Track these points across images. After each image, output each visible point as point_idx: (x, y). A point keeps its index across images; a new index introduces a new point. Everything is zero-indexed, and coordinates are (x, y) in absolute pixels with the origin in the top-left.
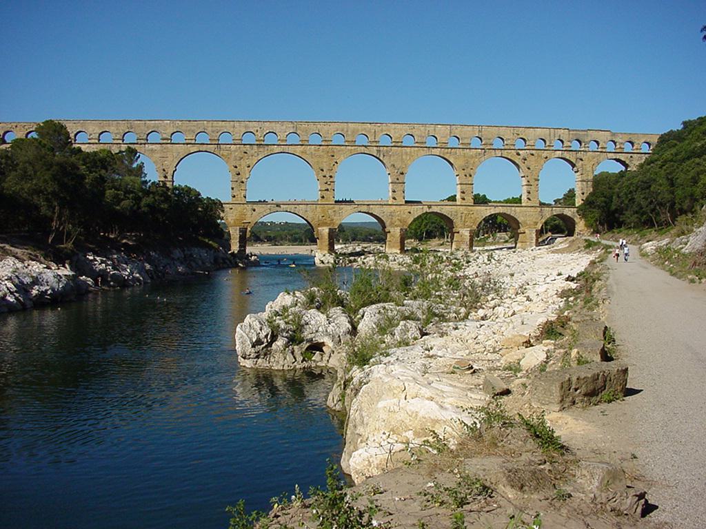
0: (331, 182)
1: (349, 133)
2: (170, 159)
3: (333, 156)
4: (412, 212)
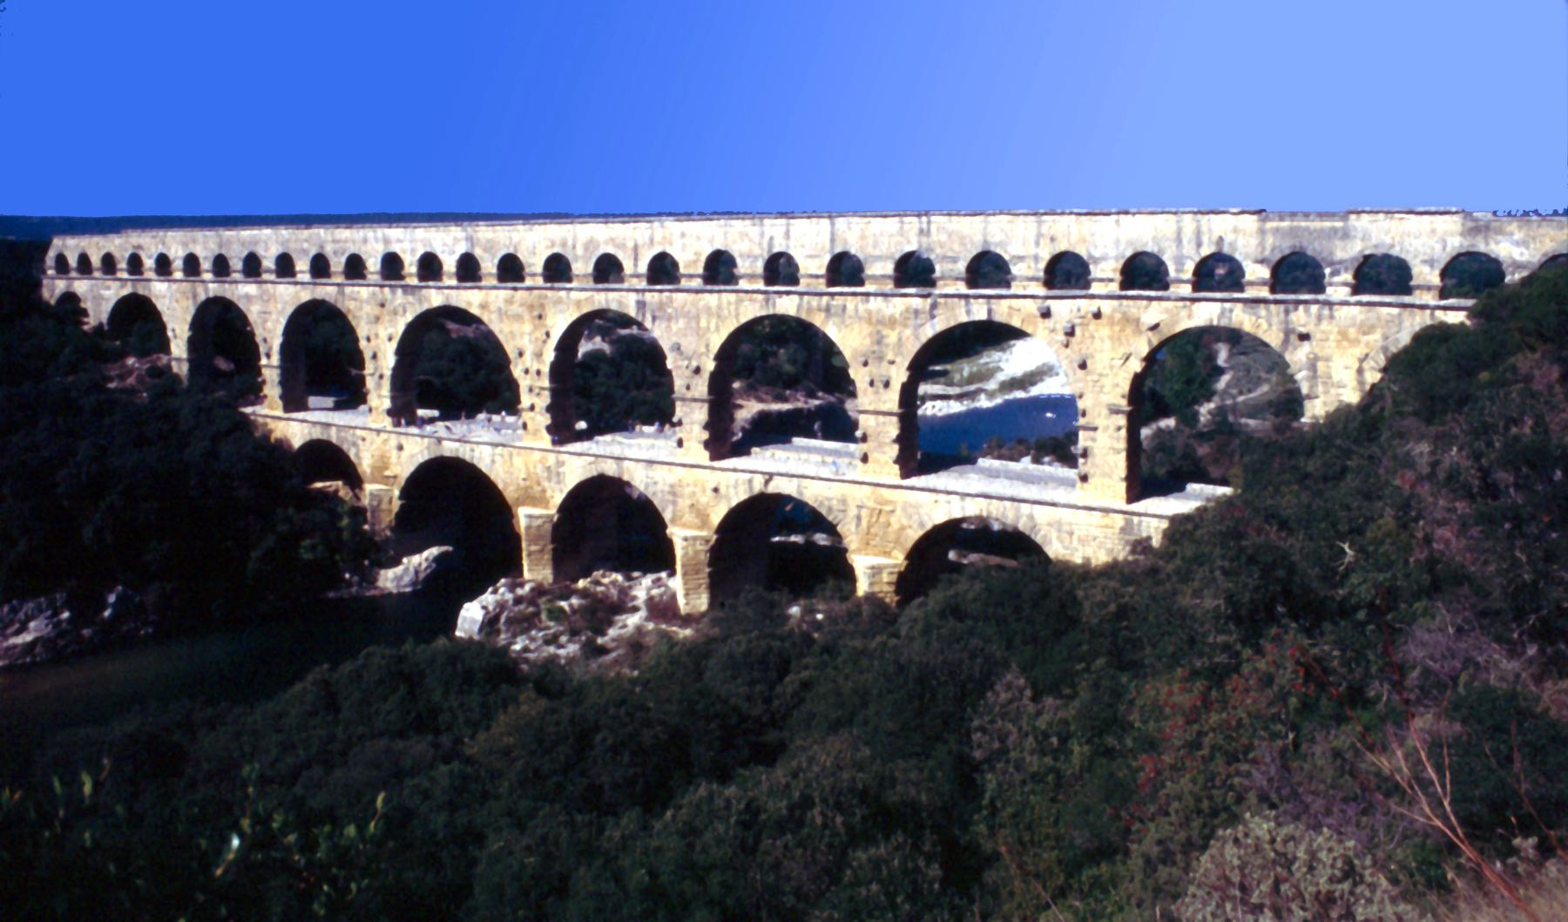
1: (580, 251)
2: (274, 317)
4: (723, 490)
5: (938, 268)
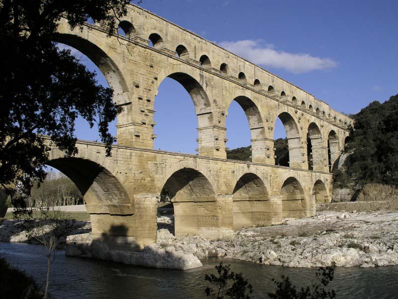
0: (151, 111)
3: (152, 67)
5: (276, 93)
